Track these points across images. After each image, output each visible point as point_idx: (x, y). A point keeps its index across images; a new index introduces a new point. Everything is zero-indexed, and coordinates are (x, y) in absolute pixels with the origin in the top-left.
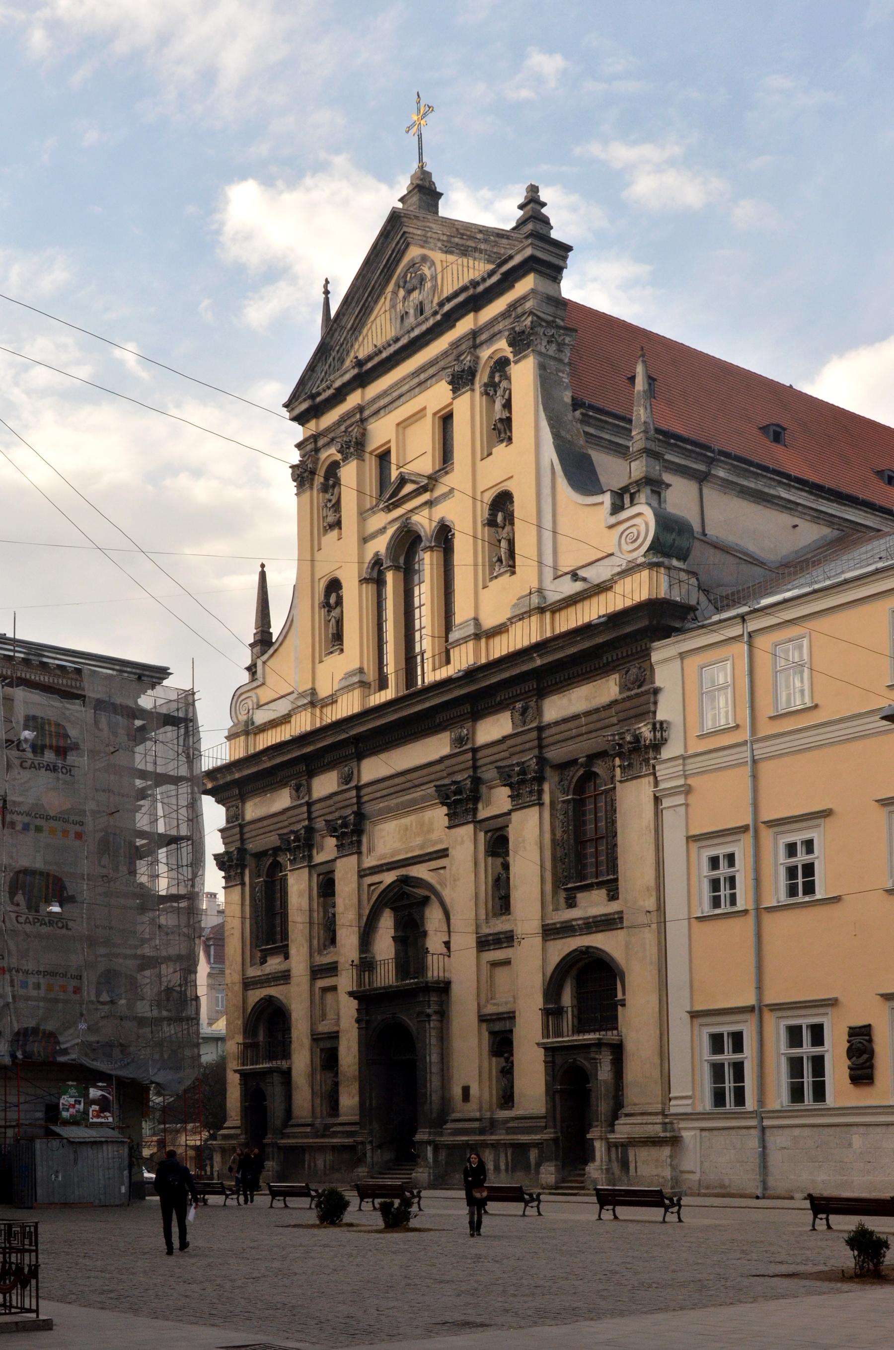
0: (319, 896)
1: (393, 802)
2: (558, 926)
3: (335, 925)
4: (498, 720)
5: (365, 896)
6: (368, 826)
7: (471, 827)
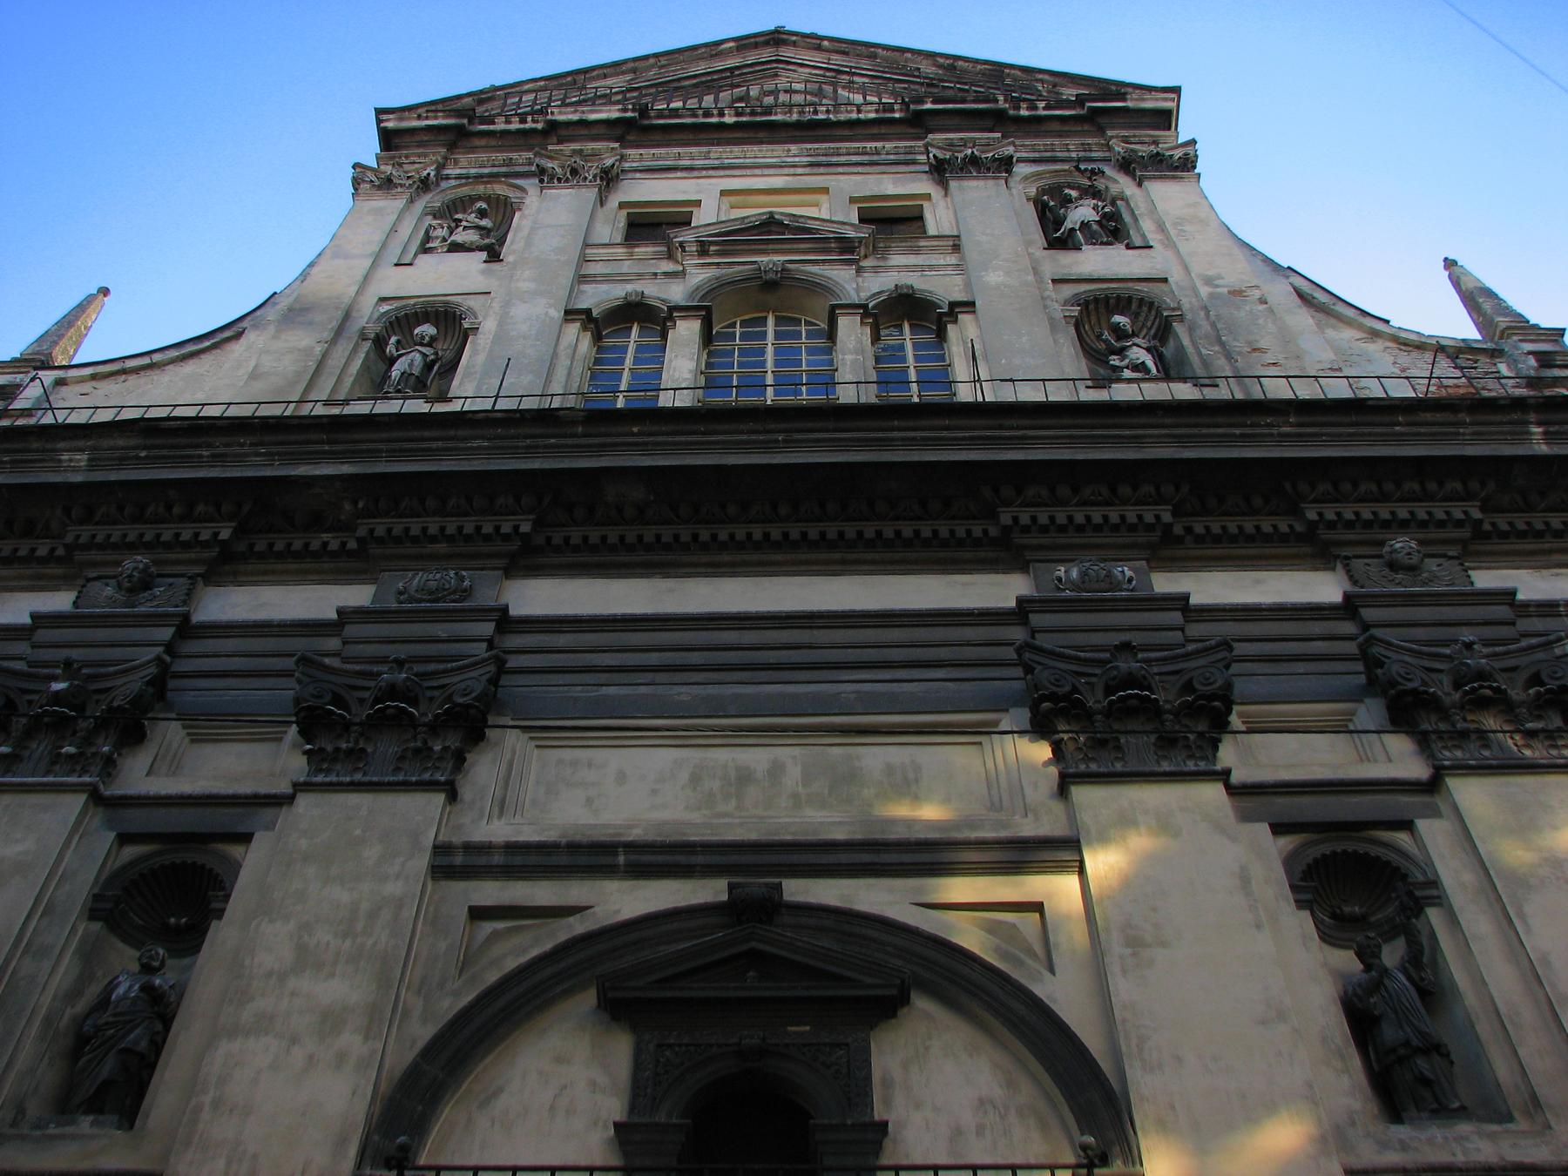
0: (93, 914)
1: (683, 693)
3: (158, 1045)
4: (1258, 582)
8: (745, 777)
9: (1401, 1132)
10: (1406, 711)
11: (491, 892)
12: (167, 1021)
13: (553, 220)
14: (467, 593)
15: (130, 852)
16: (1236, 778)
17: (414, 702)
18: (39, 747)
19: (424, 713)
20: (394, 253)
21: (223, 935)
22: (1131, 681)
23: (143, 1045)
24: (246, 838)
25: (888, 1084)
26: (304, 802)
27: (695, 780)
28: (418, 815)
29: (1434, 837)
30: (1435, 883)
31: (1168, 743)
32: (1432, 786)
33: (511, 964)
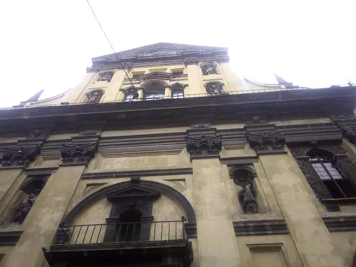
2: (342, 220)
3: (29, 210)
5: (81, 191)
6: (99, 156)
7: (217, 160)
8: (138, 161)
9: (246, 215)
10: (253, 145)
11: (91, 182)
12: (31, 206)
13: (120, 76)
14: (95, 134)
15: (30, 178)
16: (221, 157)
17: (82, 151)
18: (15, 163)
19: (85, 152)
20: (92, 81)
21: (43, 191)
22: (204, 142)
23: (26, 211)
24: (50, 175)
25: (155, 210)
26: (61, 169)
27: (130, 162)
28: (80, 170)
29: (257, 167)
30: (256, 174)
31: (209, 152)
32: (257, 158)
33: (92, 193)
